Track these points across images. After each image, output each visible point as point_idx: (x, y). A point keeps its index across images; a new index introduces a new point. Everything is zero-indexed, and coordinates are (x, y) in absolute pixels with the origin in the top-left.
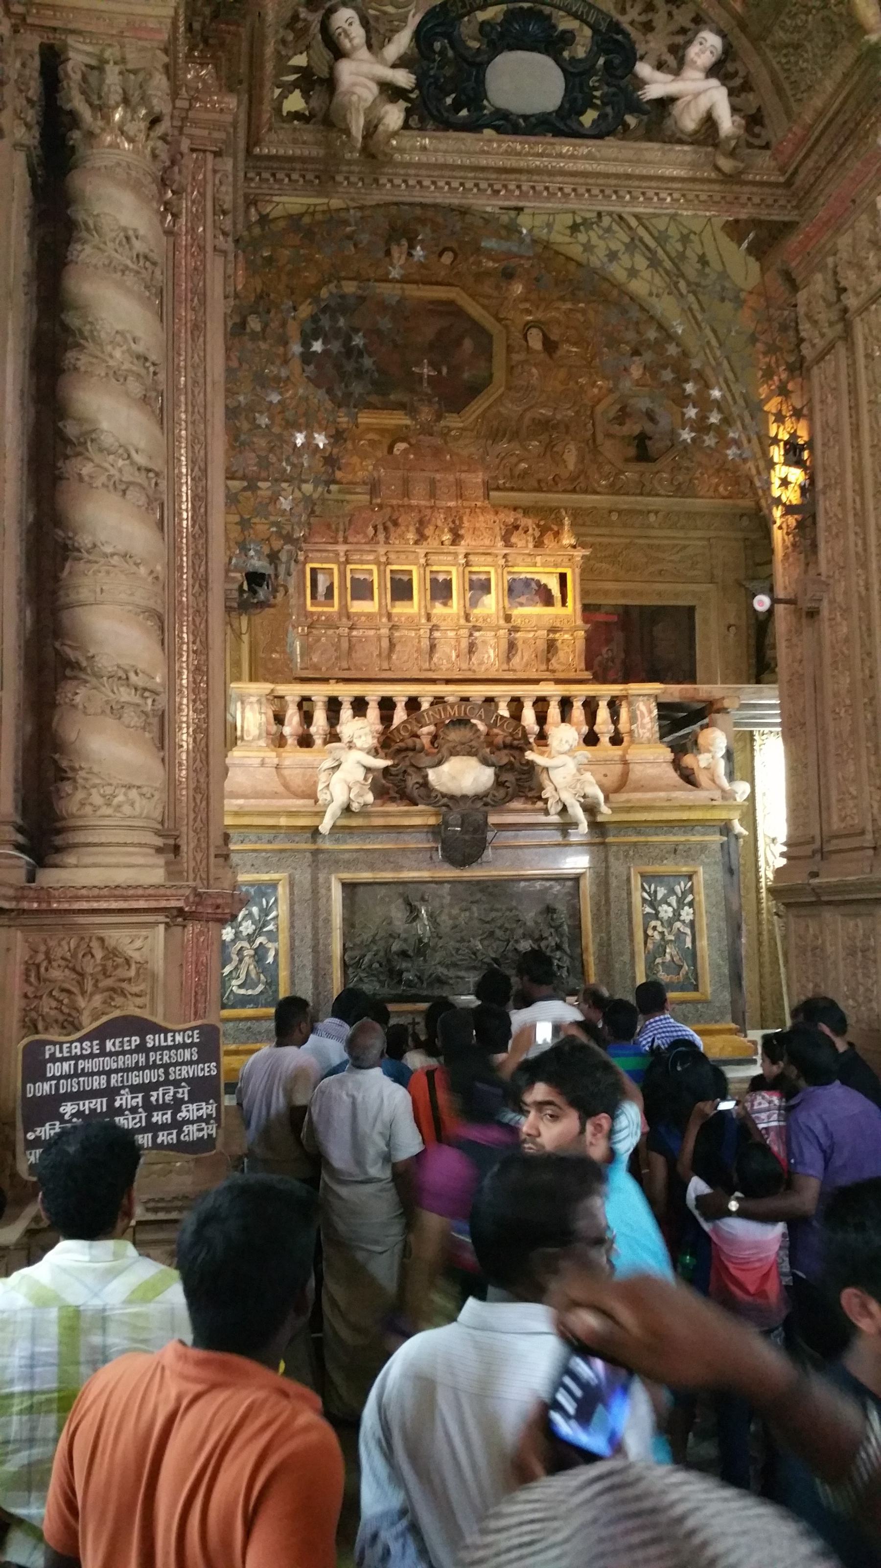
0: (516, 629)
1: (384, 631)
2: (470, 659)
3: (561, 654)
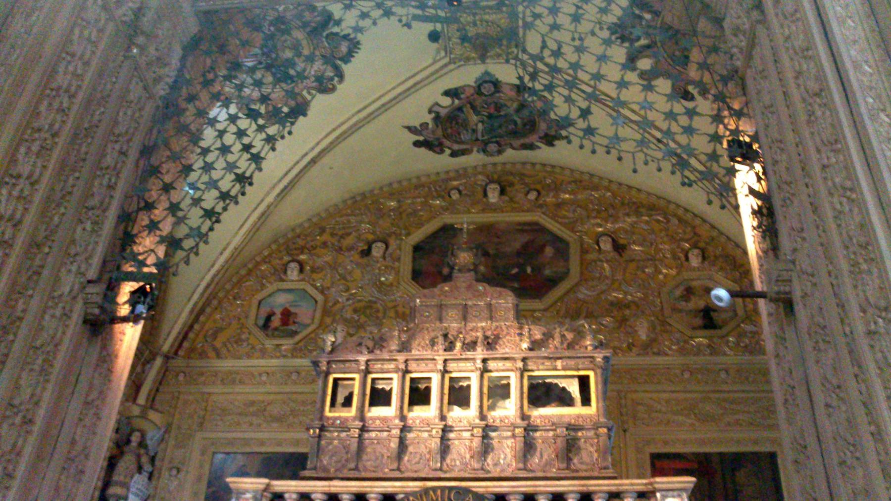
0: (535, 429)
1: (396, 432)
2: (485, 460)
3: (584, 454)
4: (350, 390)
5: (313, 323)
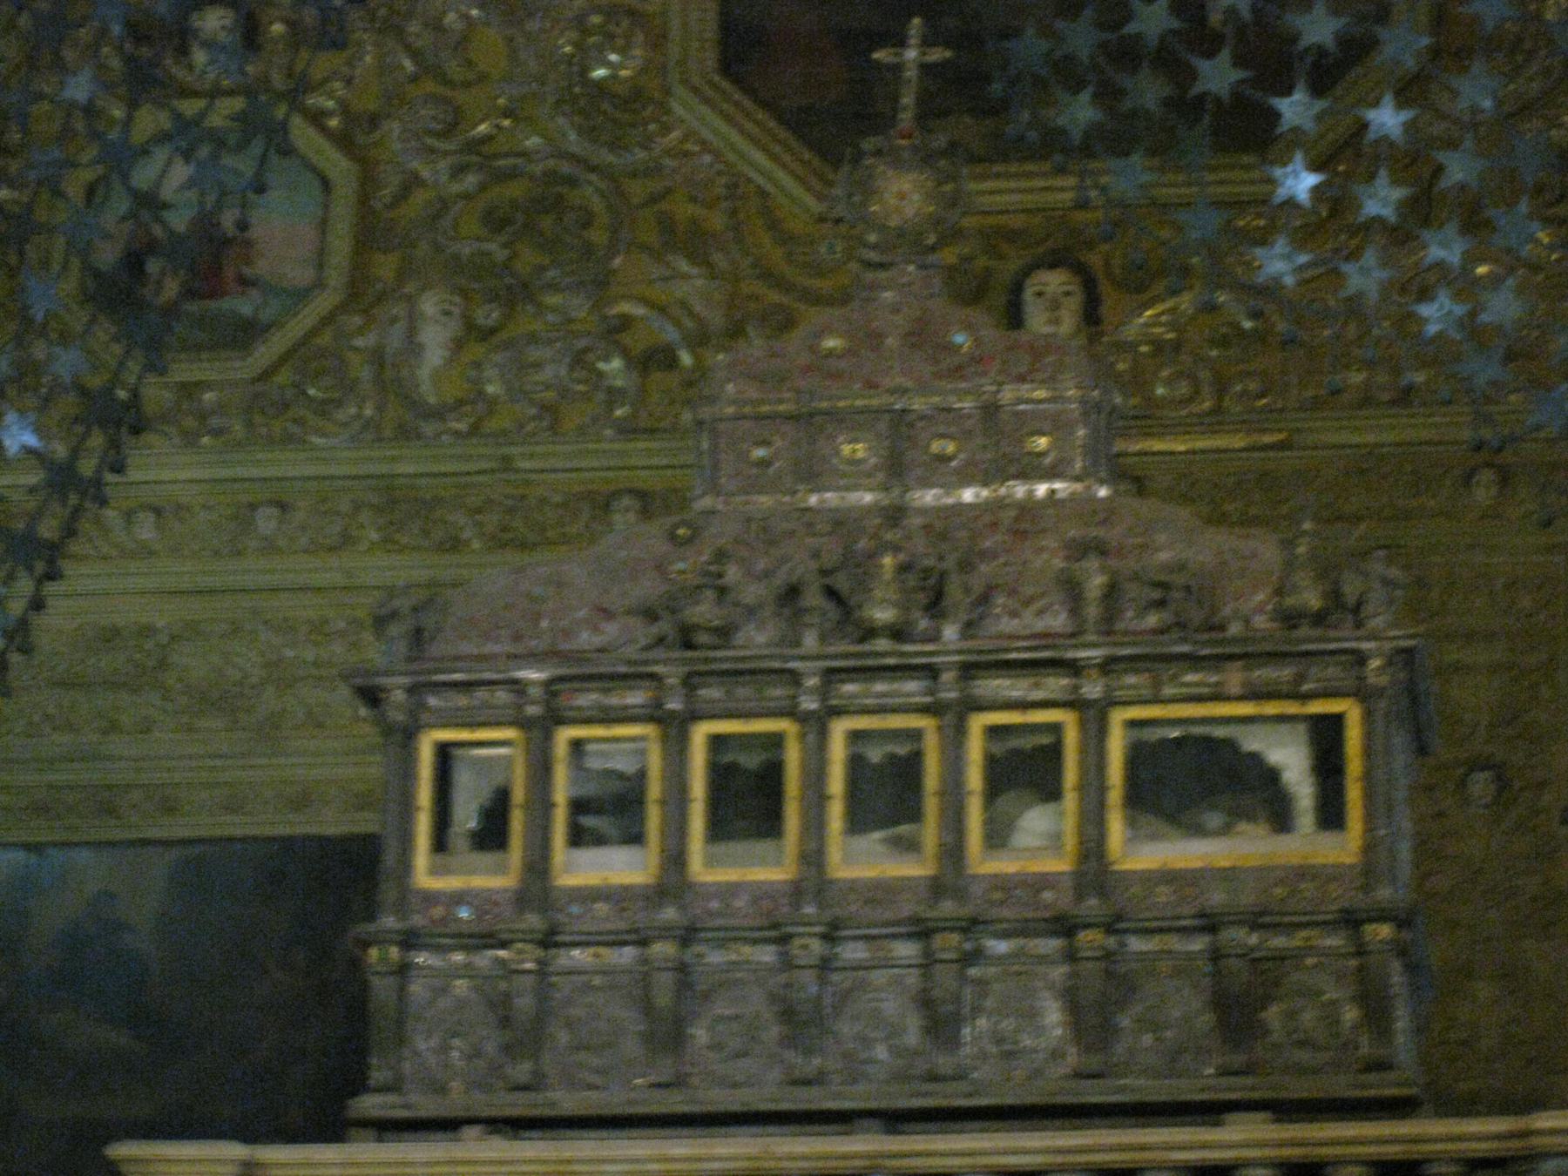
4: (499, 780)
5: (319, 284)
